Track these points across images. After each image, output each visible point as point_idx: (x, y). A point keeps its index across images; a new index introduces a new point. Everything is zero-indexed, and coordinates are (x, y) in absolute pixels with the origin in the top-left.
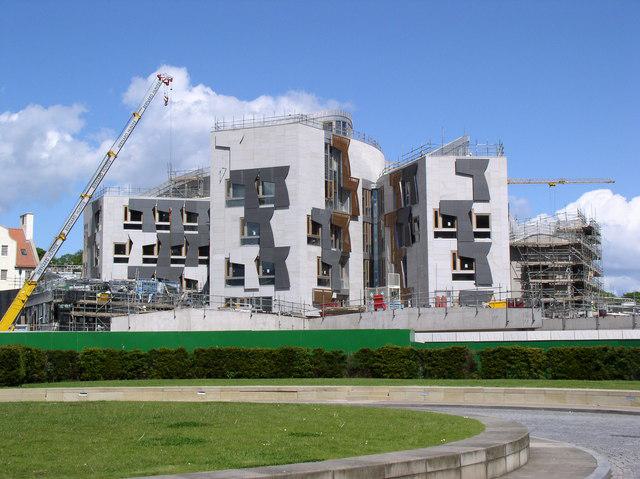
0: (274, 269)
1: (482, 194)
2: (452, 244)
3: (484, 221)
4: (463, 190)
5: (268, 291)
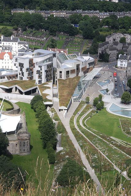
0: (23, 74)
1: (41, 70)
2: (38, 75)
3: (41, 72)
4: (39, 69)
5: (22, 76)
